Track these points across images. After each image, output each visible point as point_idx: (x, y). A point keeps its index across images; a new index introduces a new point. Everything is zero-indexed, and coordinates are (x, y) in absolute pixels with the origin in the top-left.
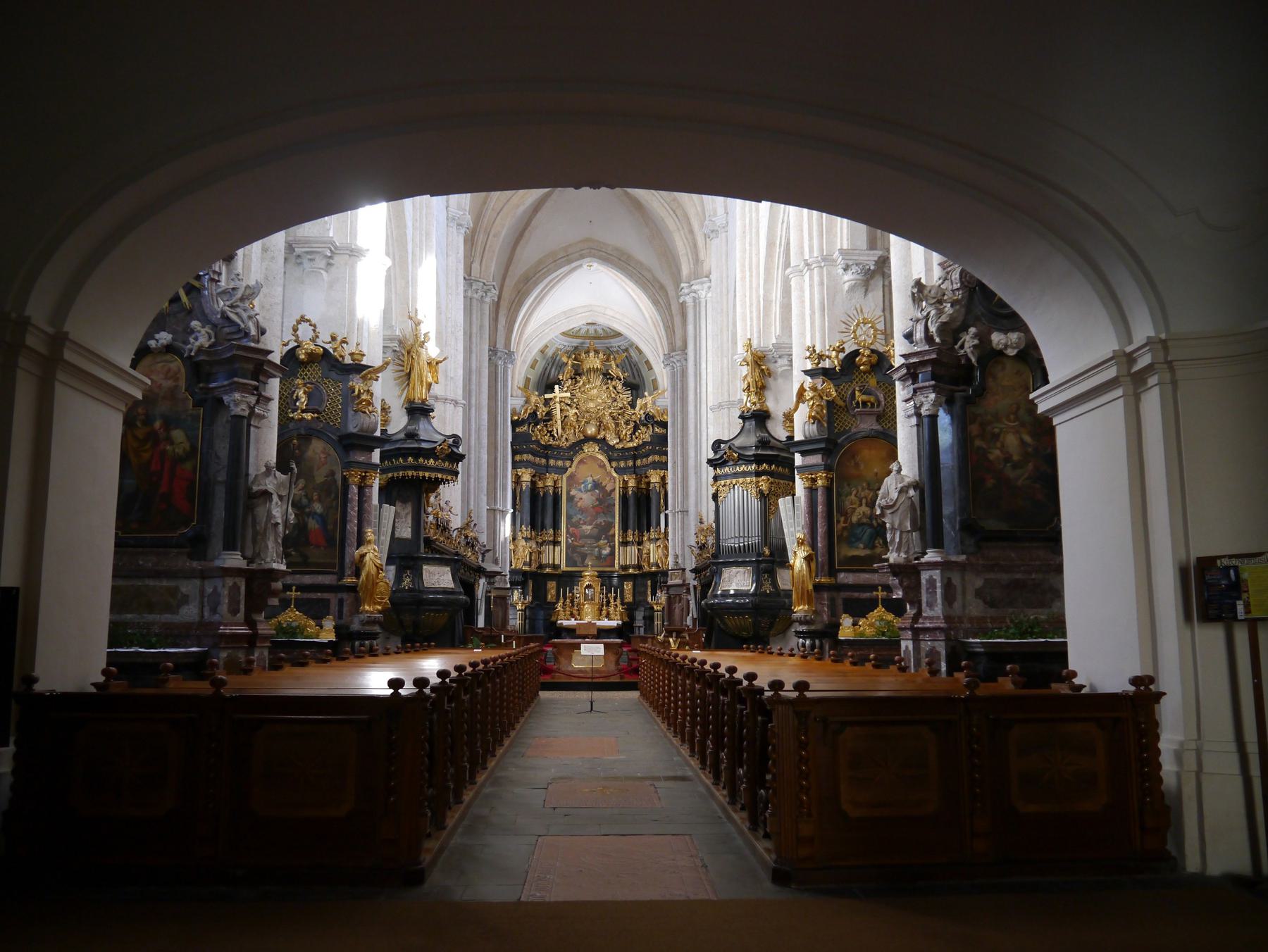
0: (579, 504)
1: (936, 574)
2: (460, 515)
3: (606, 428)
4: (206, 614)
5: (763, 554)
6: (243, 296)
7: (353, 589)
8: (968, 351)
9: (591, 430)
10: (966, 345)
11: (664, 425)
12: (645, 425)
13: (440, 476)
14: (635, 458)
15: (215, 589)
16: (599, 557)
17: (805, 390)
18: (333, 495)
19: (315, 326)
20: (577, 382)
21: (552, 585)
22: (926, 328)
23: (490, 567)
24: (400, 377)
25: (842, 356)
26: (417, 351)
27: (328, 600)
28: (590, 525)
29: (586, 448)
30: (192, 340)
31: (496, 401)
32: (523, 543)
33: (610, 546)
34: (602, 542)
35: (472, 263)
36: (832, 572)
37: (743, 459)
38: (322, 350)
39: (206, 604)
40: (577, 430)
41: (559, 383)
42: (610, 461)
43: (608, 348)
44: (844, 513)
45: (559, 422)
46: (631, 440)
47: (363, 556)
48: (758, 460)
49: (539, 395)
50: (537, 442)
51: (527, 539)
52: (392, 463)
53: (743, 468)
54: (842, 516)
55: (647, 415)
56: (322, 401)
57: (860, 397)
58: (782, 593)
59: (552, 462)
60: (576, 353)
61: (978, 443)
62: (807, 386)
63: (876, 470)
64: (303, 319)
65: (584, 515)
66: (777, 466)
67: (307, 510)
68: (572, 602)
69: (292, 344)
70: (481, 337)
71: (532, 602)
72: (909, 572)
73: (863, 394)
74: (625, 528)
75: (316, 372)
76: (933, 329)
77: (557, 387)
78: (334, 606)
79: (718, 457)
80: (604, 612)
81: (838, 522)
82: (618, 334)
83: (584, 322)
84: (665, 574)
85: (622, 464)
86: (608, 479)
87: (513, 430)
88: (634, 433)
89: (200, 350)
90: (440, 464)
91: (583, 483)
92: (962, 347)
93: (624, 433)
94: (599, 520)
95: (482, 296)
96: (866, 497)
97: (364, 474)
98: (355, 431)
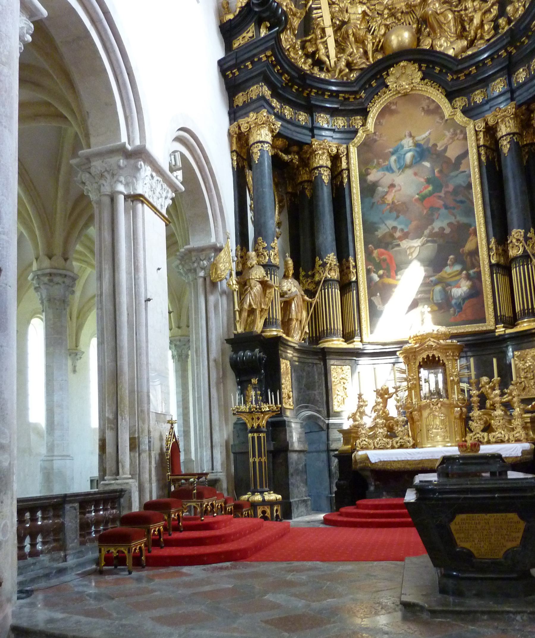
0: (389, 198)
28: (420, 237)
29: (390, 81)
32: (258, 273)
33: (468, 277)
34: (448, 270)
40: (370, 47)
42: (450, 96)
45: (329, 31)
65: (402, 217)
85: (478, 97)
86: (448, 134)
91: (393, 154)
93: (476, 21)
94: (437, 225)
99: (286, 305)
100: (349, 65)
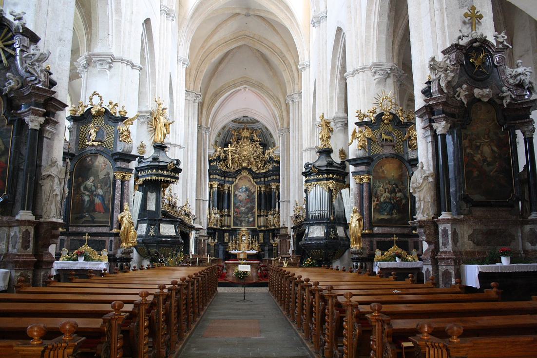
0: (239, 198)
1: (448, 226)
2: (181, 200)
3: (252, 164)
4: (10, 249)
5: (330, 219)
6: (38, 59)
7: (117, 235)
8: (463, 98)
9: (245, 165)
10: (461, 95)
11: (278, 162)
12: (269, 162)
13: (169, 179)
14: (265, 178)
15: (16, 232)
16: (248, 222)
17: (356, 133)
18: (108, 185)
19: (101, 97)
20: (238, 143)
21: (226, 234)
22: (439, 84)
23: (197, 226)
24: (151, 131)
25: (375, 115)
26: (159, 118)
27: (105, 241)
29: (242, 173)
30: (6, 84)
31: (201, 150)
32: (213, 215)
35: (190, 84)
36: (371, 227)
37: (320, 172)
38: (104, 109)
39: (10, 243)
41: (231, 143)
42: (253, 179)
43: (253, 128)
44: (377, 197)
45: (230, 161)
46: (263, 169)
47: (122, 218)
48: (328, 172)
49: (221, 149)
50: (220, 169)
51: (215, 214)
52: (146, 172)
53: (320, 176)
54: (376, 198)
55: (270, 157)
56: (104, 136)
57: (384, 137)
58: (339, 238)
59: (227, 179)
60: (238, 130)
61: (468, 151)
62: (357, 131)
63: (392, 174)
64: (95, 94)
66: (337, 175)
67: (95, 193)
68: (236, 242)
69: (90, 107)
70: (194, 118)
71: (217, 243)
72: (432, 225)
73: (386, 135)
74: (260, 208)
75: (101, 121)
76: (443, 84)
77: (229, 145)
78: (108, 244)
79: (307, 171)
80: (250, 247)
81: (374, 201)
82: (258, 122)
83: (242, 115)
84: (279, 229)
85: (259, 180)
87: (210, 164)
88: (264, 166)
89: (11, 89)
90: (169, 173)
92: (458, 96)
93: (260, 165)
94: (248, 206)
95: (194, 100)
96: (388, 188)
97: (124, 174)
98: (120, 151)
99: (217, 220)
100: (234, 168)
